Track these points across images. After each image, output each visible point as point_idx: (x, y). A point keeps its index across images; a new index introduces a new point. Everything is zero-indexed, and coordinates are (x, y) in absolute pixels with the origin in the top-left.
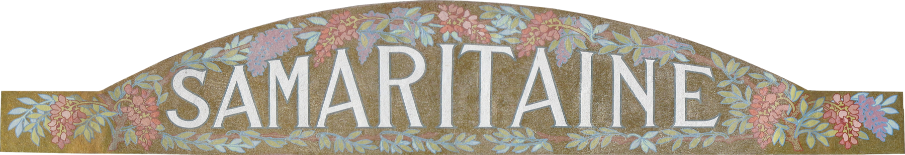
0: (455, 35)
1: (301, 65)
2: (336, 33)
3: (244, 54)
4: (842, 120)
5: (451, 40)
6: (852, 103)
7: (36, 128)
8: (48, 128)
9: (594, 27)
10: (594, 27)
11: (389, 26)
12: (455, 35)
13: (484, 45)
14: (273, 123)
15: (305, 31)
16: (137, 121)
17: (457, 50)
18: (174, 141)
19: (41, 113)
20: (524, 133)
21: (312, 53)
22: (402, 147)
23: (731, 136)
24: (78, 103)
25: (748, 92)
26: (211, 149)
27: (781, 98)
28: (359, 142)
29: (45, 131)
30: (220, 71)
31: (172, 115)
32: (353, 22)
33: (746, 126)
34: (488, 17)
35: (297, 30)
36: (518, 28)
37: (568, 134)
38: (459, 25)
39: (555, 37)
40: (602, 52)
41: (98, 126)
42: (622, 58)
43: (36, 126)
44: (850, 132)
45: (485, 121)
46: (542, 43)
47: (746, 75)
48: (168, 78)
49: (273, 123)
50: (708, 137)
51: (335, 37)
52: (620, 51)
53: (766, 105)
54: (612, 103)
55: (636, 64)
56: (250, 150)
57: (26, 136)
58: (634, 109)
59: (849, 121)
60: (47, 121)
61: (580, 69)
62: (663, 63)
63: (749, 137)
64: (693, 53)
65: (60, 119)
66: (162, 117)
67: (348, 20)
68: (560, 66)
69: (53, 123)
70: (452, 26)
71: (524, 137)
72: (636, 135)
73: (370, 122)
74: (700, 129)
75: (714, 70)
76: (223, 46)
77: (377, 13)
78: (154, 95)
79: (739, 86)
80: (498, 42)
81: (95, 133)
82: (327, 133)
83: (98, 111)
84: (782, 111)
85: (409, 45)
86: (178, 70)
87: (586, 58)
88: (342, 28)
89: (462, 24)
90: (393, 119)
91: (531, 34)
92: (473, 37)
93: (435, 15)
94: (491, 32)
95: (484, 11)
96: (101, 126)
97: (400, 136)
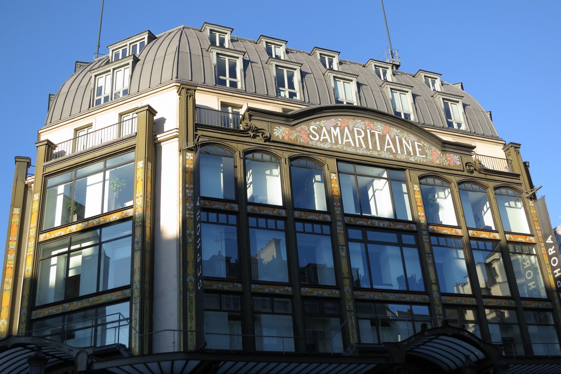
1: (338, 129)
5: (369, 129)
14: (333, 142)
17: (370, 131)
19: (281, 131)
20: (387, 153)
21: (340, 127)
29: (282, 136)
31: (311, 136)
33: (431, 158)
35: (336, 121)
40: (400, 137)
45: (379, 149)
47: (429, 147)
48: (308, 126)
53: (434, 154)
55: (407, 141)
57: (278, 136)
58: (408, 151)
60: (282, 133)
61: (396, 140)
62: (412, 141)
64: (418, 140)
66: (309, 137)
70: (368, 125)
73: (354, 145)
74: (422, 158)
75: (423, 145)
76: (320, 122)
78: (306, 131)
81: (294, 138)
86: (311, 126)
87: (397, 137)
90: (359, 145)
97: (361, 150)
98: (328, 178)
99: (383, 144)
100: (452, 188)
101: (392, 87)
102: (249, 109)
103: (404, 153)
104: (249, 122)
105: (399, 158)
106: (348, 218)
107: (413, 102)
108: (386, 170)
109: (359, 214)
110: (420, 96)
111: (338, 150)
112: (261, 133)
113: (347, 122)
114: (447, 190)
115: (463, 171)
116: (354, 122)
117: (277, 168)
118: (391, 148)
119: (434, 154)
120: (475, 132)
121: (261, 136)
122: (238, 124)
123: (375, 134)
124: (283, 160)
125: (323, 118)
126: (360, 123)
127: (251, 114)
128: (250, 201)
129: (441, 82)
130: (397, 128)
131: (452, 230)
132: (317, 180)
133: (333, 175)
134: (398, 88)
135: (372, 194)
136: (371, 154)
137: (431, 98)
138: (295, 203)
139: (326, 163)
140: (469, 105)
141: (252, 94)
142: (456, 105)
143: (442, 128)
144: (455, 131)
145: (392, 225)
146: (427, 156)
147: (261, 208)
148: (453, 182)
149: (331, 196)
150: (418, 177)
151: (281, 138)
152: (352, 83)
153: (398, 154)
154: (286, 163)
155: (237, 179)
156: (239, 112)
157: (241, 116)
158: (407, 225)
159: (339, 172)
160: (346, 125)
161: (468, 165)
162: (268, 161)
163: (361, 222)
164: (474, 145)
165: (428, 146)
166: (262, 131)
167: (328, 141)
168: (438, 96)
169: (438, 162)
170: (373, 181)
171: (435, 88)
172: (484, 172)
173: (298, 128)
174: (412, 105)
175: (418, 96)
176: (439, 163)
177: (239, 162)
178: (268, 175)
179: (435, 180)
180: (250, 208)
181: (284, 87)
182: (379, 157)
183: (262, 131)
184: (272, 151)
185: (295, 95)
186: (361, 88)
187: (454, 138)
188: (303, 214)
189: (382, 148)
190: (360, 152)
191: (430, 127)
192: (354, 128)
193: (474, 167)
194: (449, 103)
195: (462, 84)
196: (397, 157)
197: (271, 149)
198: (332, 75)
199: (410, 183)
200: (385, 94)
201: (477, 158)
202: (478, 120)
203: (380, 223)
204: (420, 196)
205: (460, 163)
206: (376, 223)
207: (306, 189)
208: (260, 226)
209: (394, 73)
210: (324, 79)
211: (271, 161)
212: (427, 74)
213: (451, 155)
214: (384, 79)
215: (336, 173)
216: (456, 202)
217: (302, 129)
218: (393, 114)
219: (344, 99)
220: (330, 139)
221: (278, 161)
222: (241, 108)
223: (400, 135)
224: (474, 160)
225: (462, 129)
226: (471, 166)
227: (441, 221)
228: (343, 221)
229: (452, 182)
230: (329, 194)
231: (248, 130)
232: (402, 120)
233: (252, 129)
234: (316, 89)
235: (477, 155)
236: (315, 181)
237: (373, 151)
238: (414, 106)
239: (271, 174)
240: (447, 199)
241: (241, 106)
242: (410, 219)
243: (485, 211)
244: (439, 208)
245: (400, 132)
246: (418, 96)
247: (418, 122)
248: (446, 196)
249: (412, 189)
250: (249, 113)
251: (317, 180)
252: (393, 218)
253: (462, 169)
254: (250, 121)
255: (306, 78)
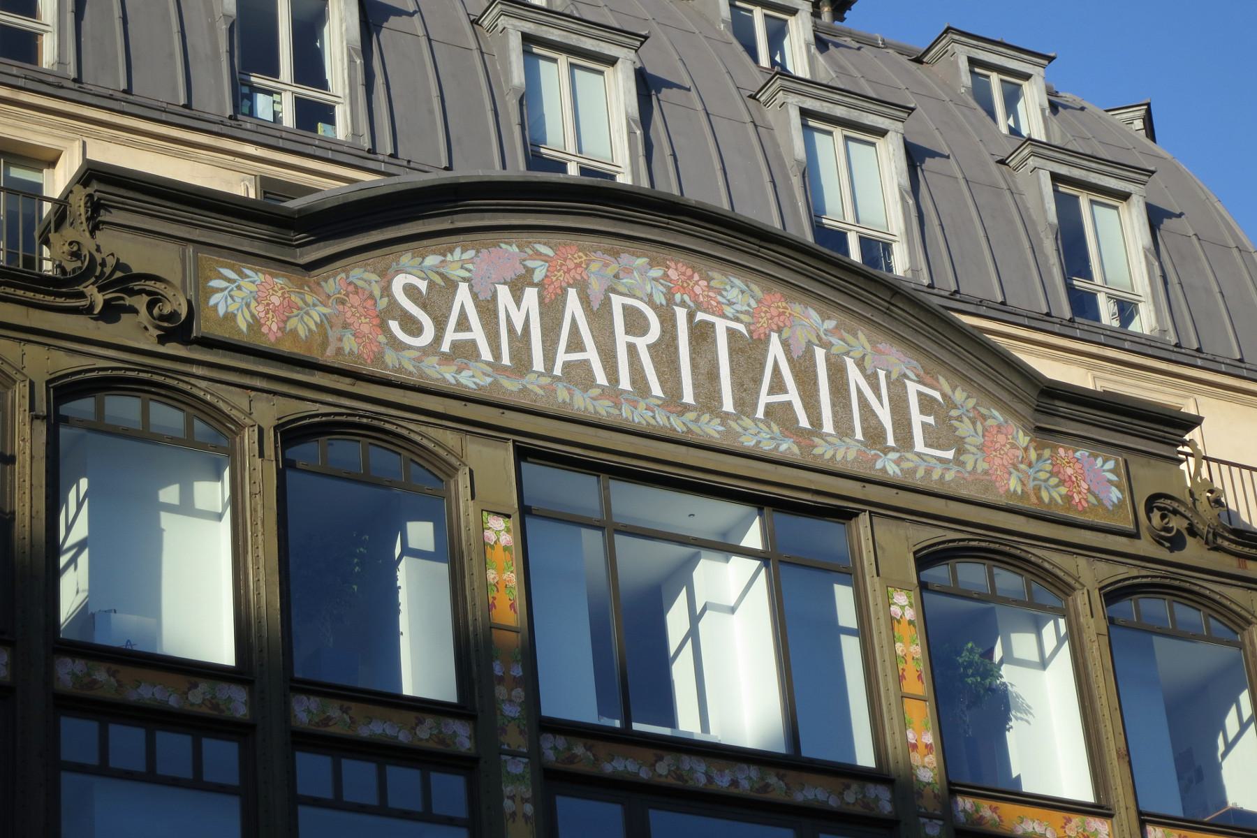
0: (686, 298)
1: (531, 295)
2: (565, 268)
3: (469, 271)
4: (1070, 477)
5: (683, 304)
6: (1075, 460)
7: (242, 311)
8: (256, 313)
9: (823, 321)
10: (823, 321)
11: (618, 273)
12: (686, 298)
13: (717, 316)
14: (506, 360)
15: (531, 258)
16: (356, 325)
17: (691, 316)
18: (398, 359)
20: (769, 427)
21: (540, 285)
22: (645, 416)
23: (969, 473)
24: (288, 289)
25: (979, 427)
26: (440, 377)
27: (1011, 441)
28: (600, 402)
29: (253, 316)
30: (443, 284)
31: (394, 326)
32: (581, 260)
33: (982, 466)
34: (718, 286)
35: (523, 255)
36: (749, 305)
37: (813, 438)
38: (690, 287)
39: (787, 324)
41: (313, 322)
42: (854, 361)
43: (241, 307)
44: (1080, 493)
45: (728, 405)
46: (775, 327)
47: (974, 408)
48: (386, 277)
49: (506, 360)
50: (948, 469)
51: (565, 273)
52: (851, 354)
53: (998, 446)
54: (851, 411)
55: (869, 372)
56: (482, 386)
57: (230, 317)
58: (872, 423)
59: (1077, 480)
60: (253, 304)
62: (894, 376)
63: (987, 478)
64: (922, 372)
65: (268, 304)
67: (576, 256)
68: (795, 357)
69: (261, 308)
70: (684, 288)
71: (769, 432)
72: (879, 452)
73: (609, 381)
74: (940, 460)
75: (944, 395)
76: (445, 256)
77: (605, 255)
78: (371, 296)
79: (970, 418)
80: (731, 315)
81: (310, 330)
82: (565, 384)
83: (311, 304)
84: (1014, 455)
85: (641, 299)
86: (398, 272)
87: (820, 354)
88: (571, 264)
89: (693, 287)
90: (633, 382)
91: (763, 315)
92: (705, 306)
93: (665, 271)
94: (723, 303)
95: (714, 279)
96: (316, 323)
97: (642, 405)
98: (468, 540)
99: (751, 385)
100: (1077, 615)
101: (810, 104)
102: (92, 174)
103: (853, 431)
104: (85, 239)
105: (827, 456)
106: (561, 741)
107: (906, 182)
108: (761, 514)
109: (617, 724)
110: (942, 156)
111: (525, 402)
112: (145, 299)
113: (578, 265)
114: (1051, 625)
115: (1135, 535)
116: (613, 268)
117: (218, 477)
118: (789, 404)
119: (998, 446)
120: (1199, 350)
121: (143, 310)
122: (29, 244)
123: (714, 331)
124: (249, 439)
125: (462, 237)
126: (643, 273)
127: (99, 199)
128: (75, 636)
129: (1051, 93)
130: (824, 307)
131: (1069, 821)
132: (413, 544)
133: (497, 524)
134: (840, 112)
135: (686, 626)
136: (690, 431)
137: (994, 168)
138: (299, 656)
139: (466, 465)
140: (1180, 215)
141: (111, 97)
142: (1115, 212)
143: (1043, 321)
144: (1102, 339)
145: (778, 787)
146: (960, 451)
147: (127, 673)
148: (1083, 586)
149: (480, 630)
150: (915, 553)
151: (244, 327)
152: (615, 73)
153: (822, 436)
154: (261, 455)
155: (14, 519)
156: (39, 186)
157: (47, 207)
158: (848, 787)
159: (525, 511)
160: (574, 279)
161: (1159, 509)
162: (174, 441)
163: (621, 765)
164: (1193, 411)
165: (971, 403)
166: (150, 285)
167: (479, 355)
168: (1032, 162)
169: (1014, 484)
170: (691, 563)
171: (1017, 121)
172: (1233, 547)
173: (331, 281)
174: (903, 199)
175: (934, 154)
176: (1019, 492)
177: (28, 437)
178: (170, 508)
179: (996, 570)
180: (68, 672)
181: (274, 72)
182: (726, 444)
183: (150, 285)
184: (195, 391)
185: (326, 113)
186: (654, 98)
187: (1099, 374)
188: (334, 710)
189: (745, 403)
190: (638, 416)
191: (983, 310)
192: (613, 296)
193: (1187, 518)
194: (1084, 200)
195: (1149, 111)
196: (817, 451)
197: (193, 381)
198: (515, 27)
199: (873, 585)
200: (773, 139)
201: (1204, 471)
202: (1216, 289)
203: (714, 773)
204: (918, 649)
205: (1120, 496)
206: (699, 773)
207: (355, 587)
208: (114, 763)
209: (824, 36)
210: (473, 45)
211: (187, 441)
212: (984, 49)
213: (1078, 454)
214: (773, 63)
215: (509, 516)
216: (1094, 686)
217: (351, 288)
218: (809, 238)
219: (571, 148)
220: (490, 345)
221: (225, 443)
222: (52, 164)
223: (834, 340)
224: (1189, 484)
225: (1139, 330)
226: (1175, 512)
227: (1014, 775)
228: (534, 754)
229: (1077, 585)
230: (470, 617)
231: (83, 276)
232: (850, 269)
233: (102, 273)
234: (435, 92)
235: (1205, 458)
236: (407, 551)
237: (699, 416)
238: (911, 202)
239: (186, 507)
240: (1049, 669)
241: (50, 157)
242: (865, 757)
243: (1231, 737)
244: (1008, 710)
245: (836, 327)
246: (934, 154)
247: (926, 281)
248: (1048, 652)
249: (881, 614)
250: (89, 190)
251: (413, 544)
252: (781, 748)
253: (1130, 526)
254: (92, 233)
255: (384, 34)
